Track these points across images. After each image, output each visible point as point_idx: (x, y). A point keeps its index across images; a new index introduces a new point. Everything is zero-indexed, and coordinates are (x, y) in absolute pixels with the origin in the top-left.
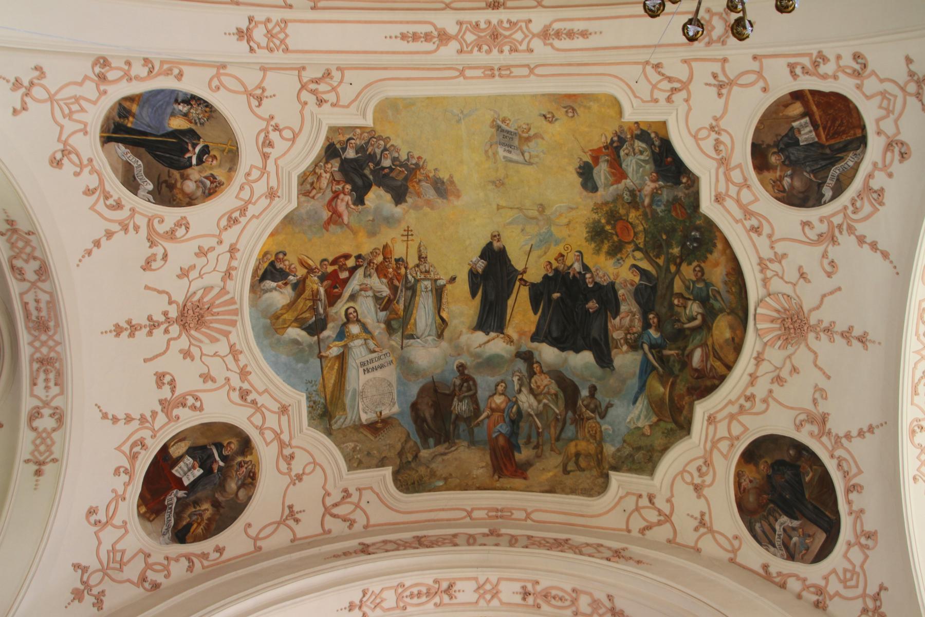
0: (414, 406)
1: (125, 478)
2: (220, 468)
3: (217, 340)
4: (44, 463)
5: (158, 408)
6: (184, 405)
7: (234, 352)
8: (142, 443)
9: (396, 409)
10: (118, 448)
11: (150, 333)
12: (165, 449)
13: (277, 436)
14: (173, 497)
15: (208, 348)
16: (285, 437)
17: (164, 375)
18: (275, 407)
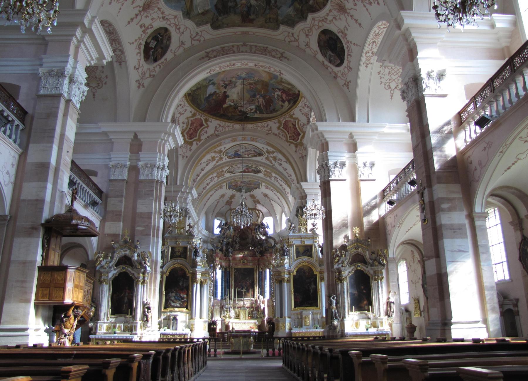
0: (216, 6)
1: (139, 55)
2: (161, 39)
3: (154, 9)
4: (121, 62)
5: (142, 33)
6: (148, 29)
7: (159, 9)
8: (141, 44)
9: (210, 7)
10: (136, 49)
11: (137, 18)
12: (146, 42)
13: (175, 24)
14: (151, 53)
15: (152, 12)
16: (177, 24)
17: (142, 25)
18: (173, 17)
